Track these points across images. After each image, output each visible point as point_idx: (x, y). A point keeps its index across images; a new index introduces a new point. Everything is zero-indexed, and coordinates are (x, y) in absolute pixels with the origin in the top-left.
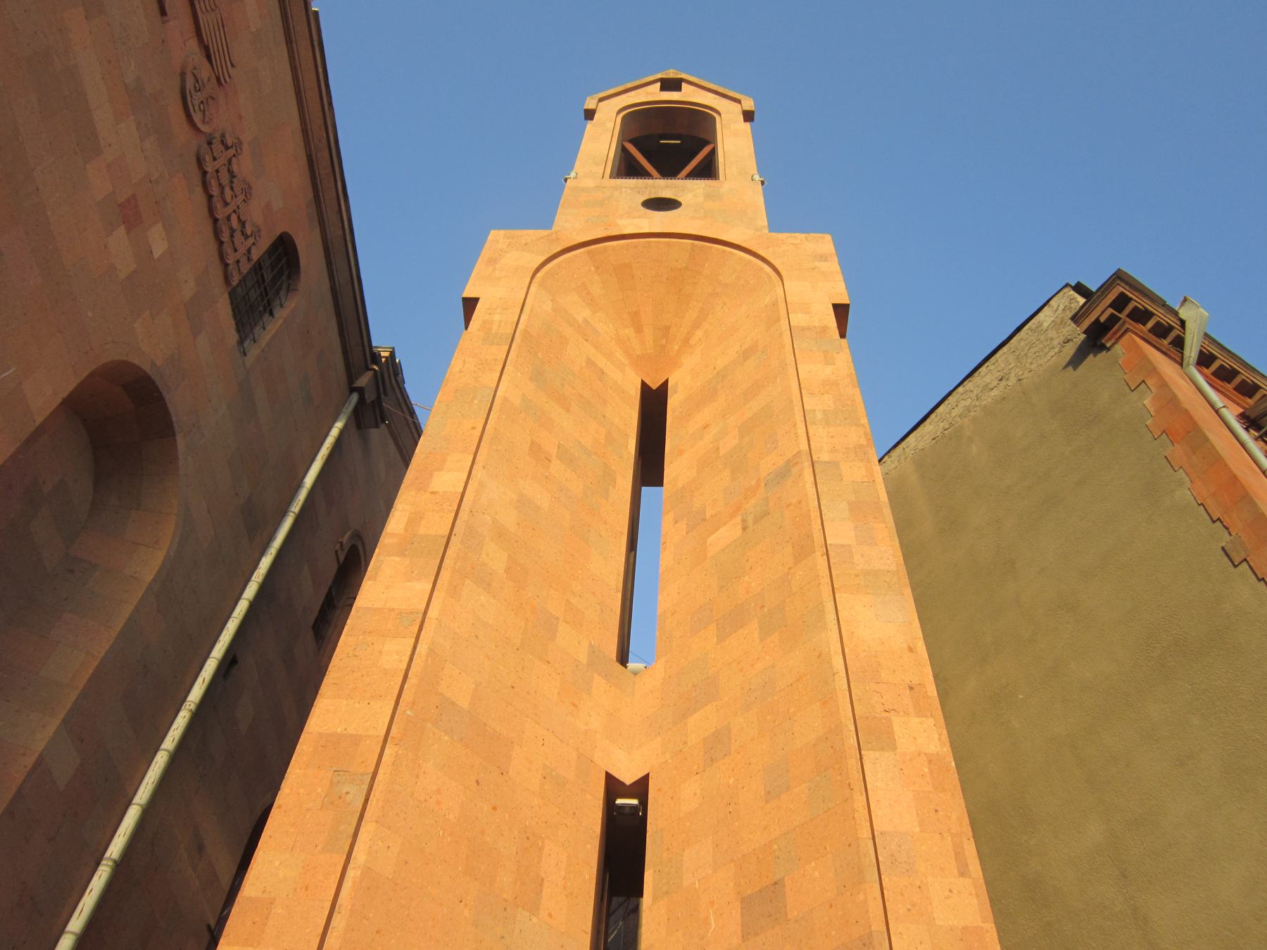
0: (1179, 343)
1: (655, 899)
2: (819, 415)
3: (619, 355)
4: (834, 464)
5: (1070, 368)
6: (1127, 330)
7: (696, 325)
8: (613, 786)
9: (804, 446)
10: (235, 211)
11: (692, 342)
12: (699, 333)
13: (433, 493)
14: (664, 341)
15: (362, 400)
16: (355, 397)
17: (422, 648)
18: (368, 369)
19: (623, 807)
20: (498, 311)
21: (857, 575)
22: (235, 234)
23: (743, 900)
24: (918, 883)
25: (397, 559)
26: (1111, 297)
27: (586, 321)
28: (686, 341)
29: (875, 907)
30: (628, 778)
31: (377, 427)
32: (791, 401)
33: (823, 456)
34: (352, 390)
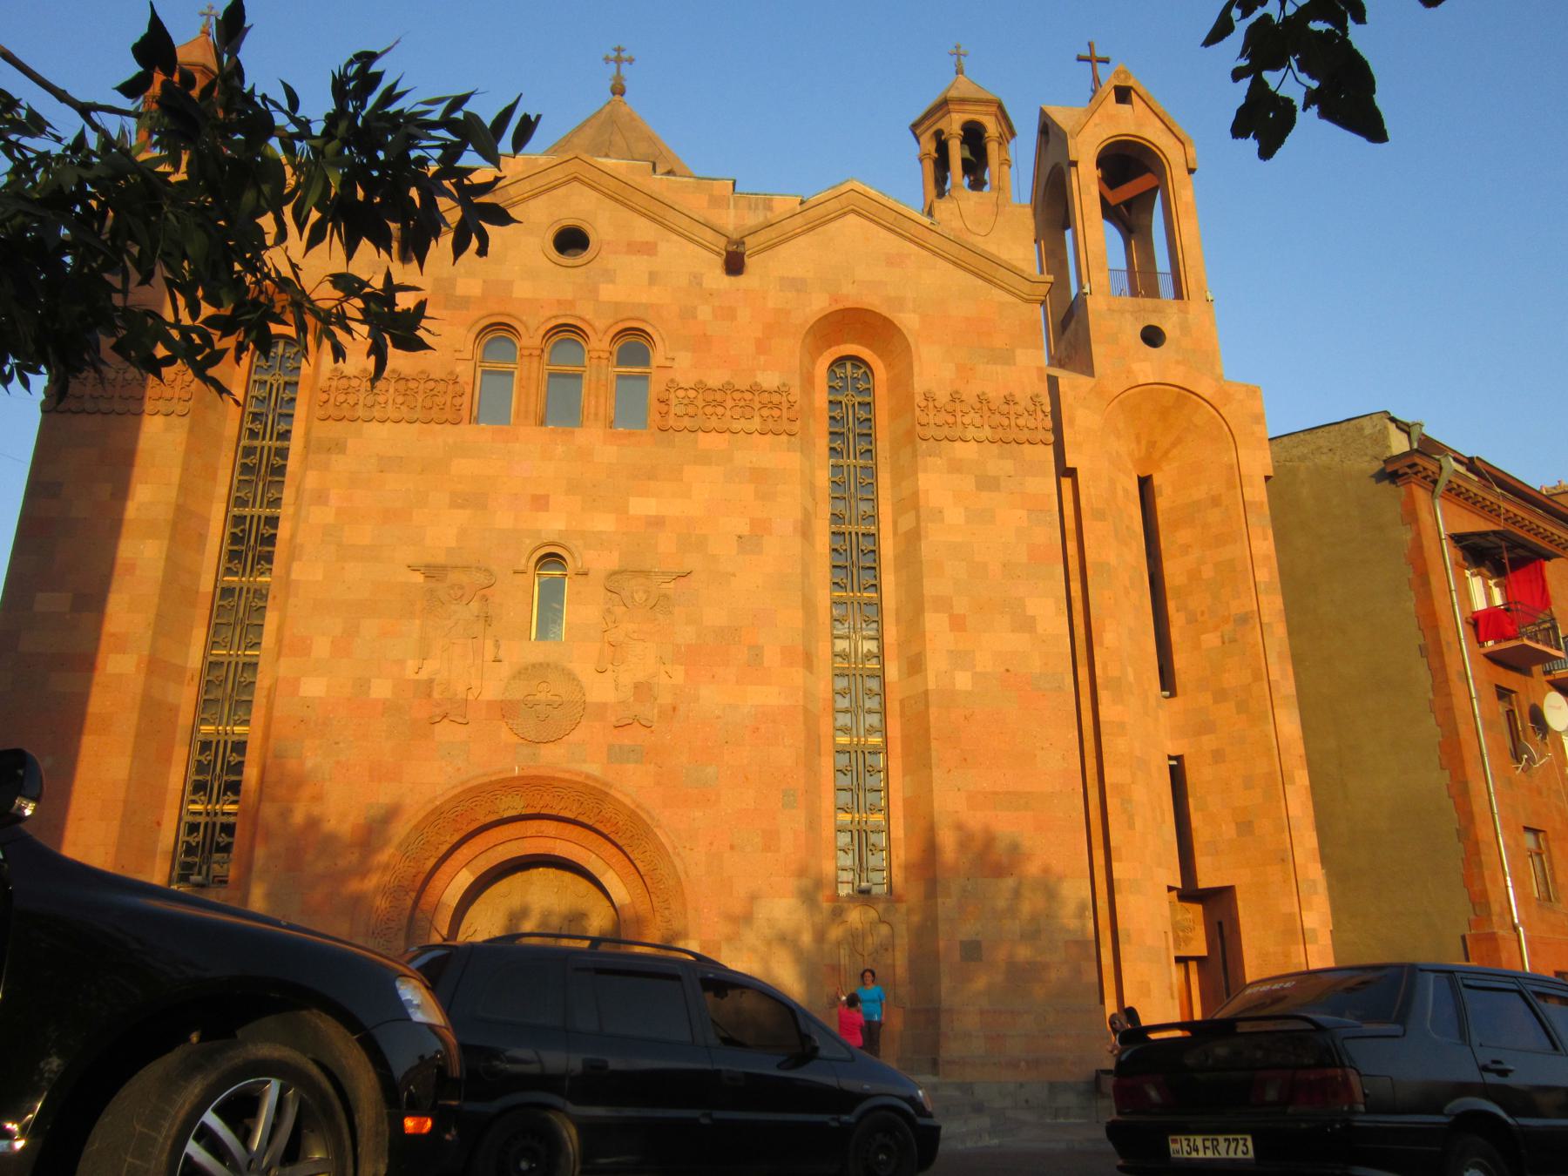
0: (1435, 482)
1: (1195, 810)
3: (1130, 466)
4: (1269, 625)
5: (1373, 479)
6: (1411, 482)
7: (1174, 445)
8: (1170, 758)
9: (1255, 608)
11: (1170, 456)
12: (1175, 452)
13: (1107, 648)
14: (1151, 450)
20: (1091, 483)
23: (1237, 823)
25: (1105, 692)
26: (1408, 462)
27: (1117, 453)
28: (1166, 453)
29: (1288, 840)
30: (1172, 754)
32: (1247, 568)
33: (1265, 619)
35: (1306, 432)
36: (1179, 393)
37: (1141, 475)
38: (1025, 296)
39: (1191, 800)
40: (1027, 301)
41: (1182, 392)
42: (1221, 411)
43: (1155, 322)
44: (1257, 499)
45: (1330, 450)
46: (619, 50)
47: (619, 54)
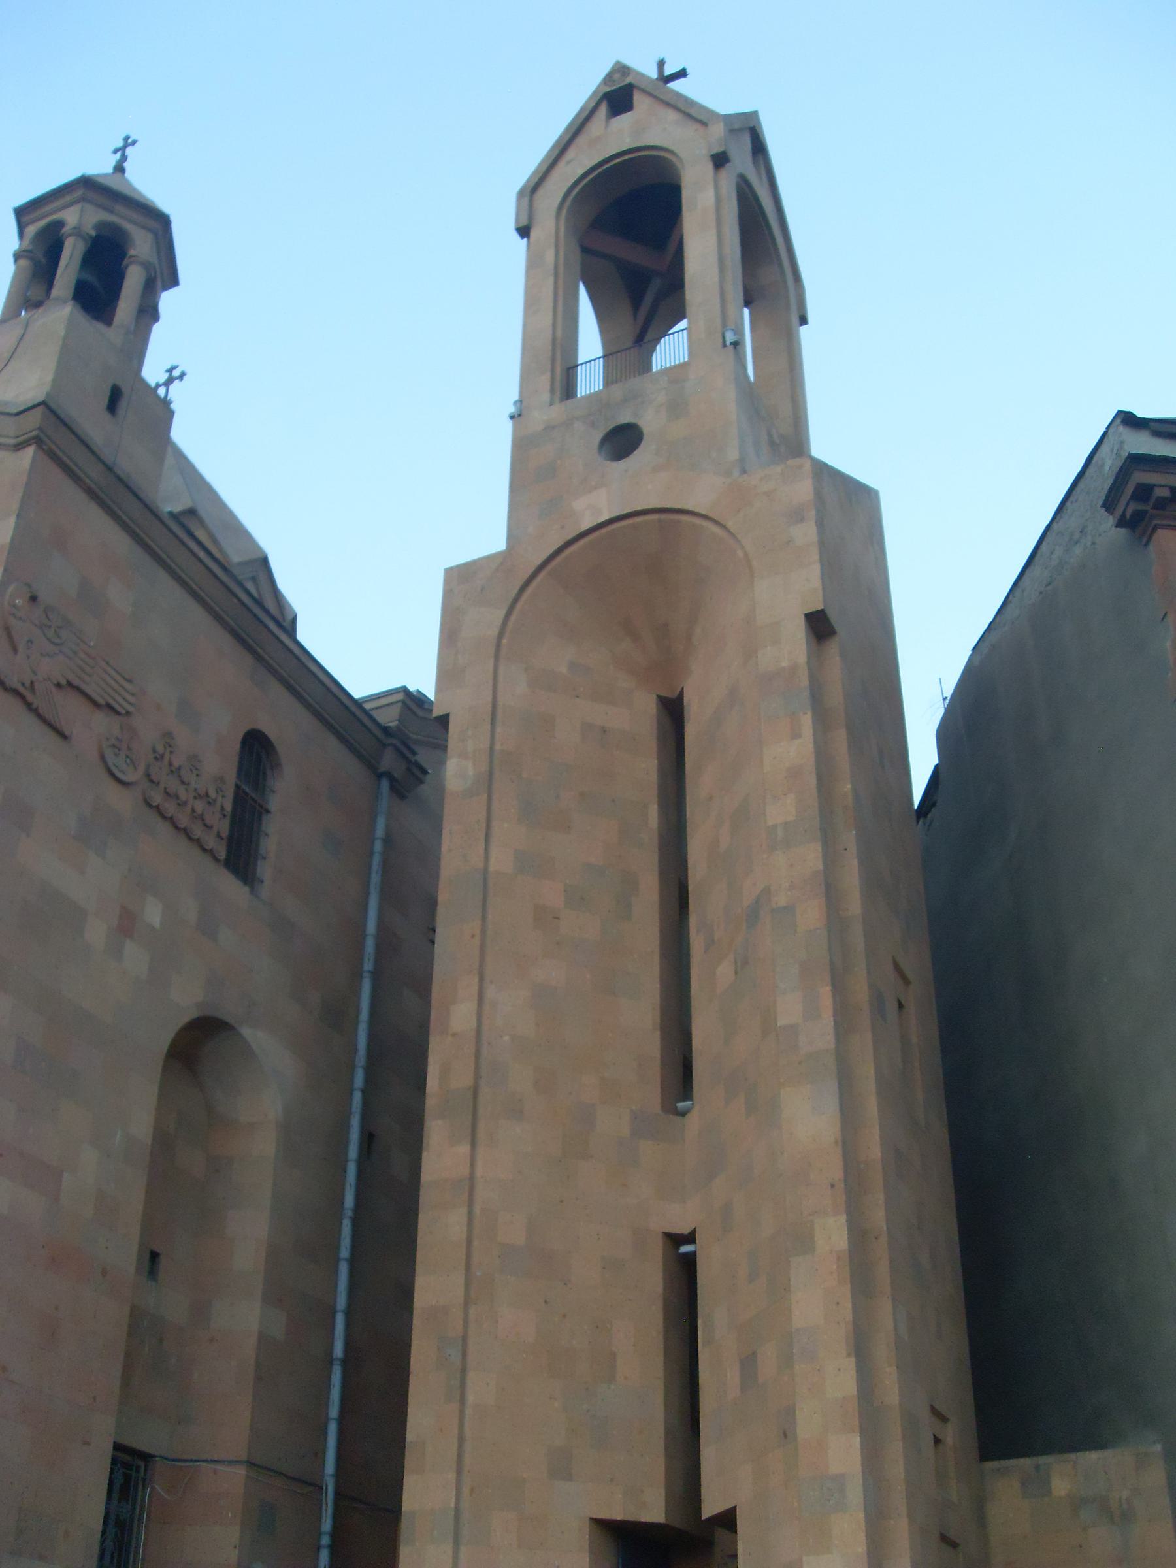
2: (780, 833)
4: (789, 909)
8: (675, 1240)
10: (195, 798)
13: (454, 1035)
15: (392, 780)
16: (385, 784)
17: (477, 1210)
18: (385, 746)
19: (685, 1254)
21: (800, 1063)
22: (208, 821)
24: (818, 1368)
25: (440, 1122)
30: (685, 1230)
31: (422, 782)
34: (379, 776)
35: (1058, 518)
36: (660, 521)
37: (664, 694)
38: (13, 441)
39: (700, 1322)
40: (19, 447)
41: (664, 516)
42: (730, 524)
43: (625, 418)
44: (785, 664)
45: (1081, 532)
46: (170, 371)
47: (171, 375)
